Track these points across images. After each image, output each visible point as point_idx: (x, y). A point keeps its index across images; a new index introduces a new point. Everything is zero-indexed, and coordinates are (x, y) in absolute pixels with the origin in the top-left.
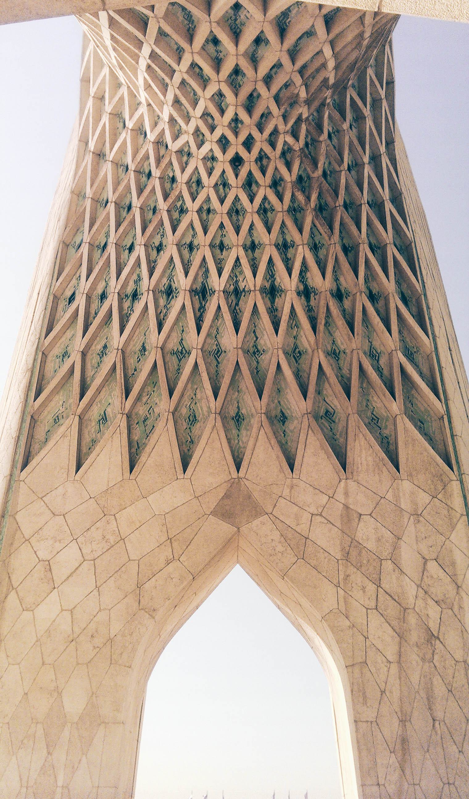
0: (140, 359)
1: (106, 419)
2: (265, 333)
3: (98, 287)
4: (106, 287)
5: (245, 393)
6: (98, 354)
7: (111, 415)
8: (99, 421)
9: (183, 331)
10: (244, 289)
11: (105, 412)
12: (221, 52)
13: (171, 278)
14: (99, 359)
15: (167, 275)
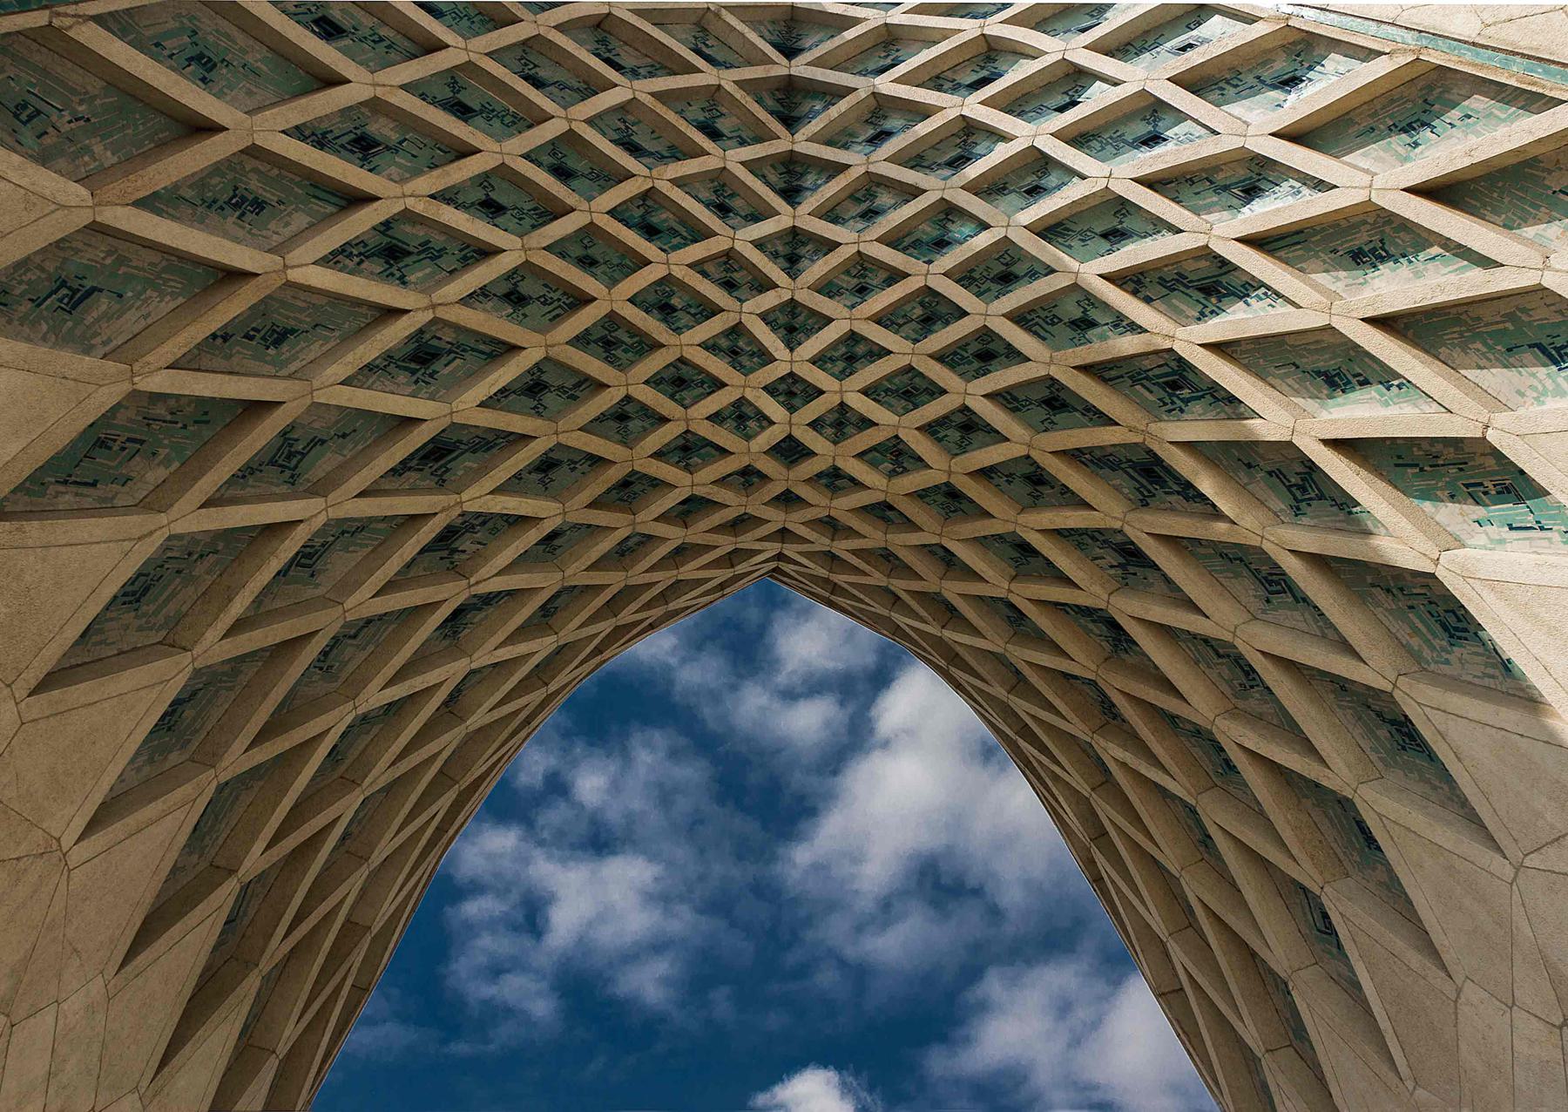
0: (251, 338)
1: (74, 308)
2: (371, 648)
3: (383, 120)
4: (388, 148)
5: (231, 689)
6: (236, 188)
7: (89, 320)
8: (64, 284)
9: (344, 436)
10: (456, 550)
11: (93, 290)
12: (1009, 482)
13: (457, 350)
14: (225, 197)
15: (462, 339)
